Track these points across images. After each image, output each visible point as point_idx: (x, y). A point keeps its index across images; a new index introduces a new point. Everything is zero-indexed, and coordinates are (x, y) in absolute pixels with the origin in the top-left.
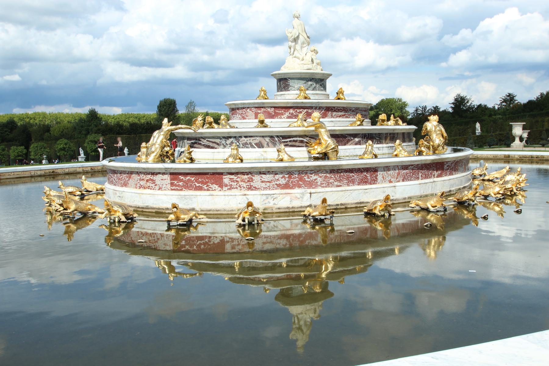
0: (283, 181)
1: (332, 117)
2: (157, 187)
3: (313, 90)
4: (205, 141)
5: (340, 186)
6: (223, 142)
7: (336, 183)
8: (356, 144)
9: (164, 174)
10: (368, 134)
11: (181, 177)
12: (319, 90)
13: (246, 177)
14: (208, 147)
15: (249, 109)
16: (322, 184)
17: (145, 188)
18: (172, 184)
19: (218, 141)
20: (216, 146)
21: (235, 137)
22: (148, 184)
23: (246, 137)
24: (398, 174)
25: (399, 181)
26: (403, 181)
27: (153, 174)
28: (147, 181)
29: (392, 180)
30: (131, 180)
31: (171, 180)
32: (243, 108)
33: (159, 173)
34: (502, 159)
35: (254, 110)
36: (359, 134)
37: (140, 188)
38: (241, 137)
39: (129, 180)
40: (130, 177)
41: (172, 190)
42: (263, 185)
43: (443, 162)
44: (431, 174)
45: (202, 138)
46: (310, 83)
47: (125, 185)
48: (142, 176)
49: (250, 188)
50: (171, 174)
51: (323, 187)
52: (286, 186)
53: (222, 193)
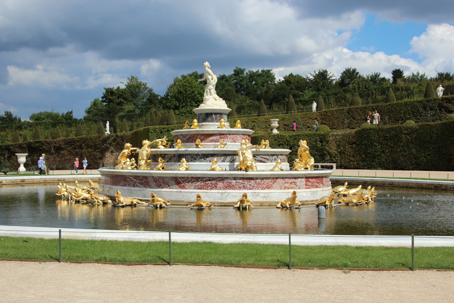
2: (297, 187)
4: (259, 157)
6: (271, 158)
9: (302, 178)
11: (310, 180)
14: (261, 161)
15: (238, 136)
17: (288, 188)
18: (306, 185)
19: (267, 157)
20: (266, 161)
21: (276, 155)
22: (291, 185)
23: (281, 155)
27: (295, 178)
28: (291, 183)
30: (275, 184)
31: (306, 181)
32: (235, 134)
33: (299, 177)
34: (97, 181)
35: (241, 136)
37: (284, 189)
38: (279, 155)
39: (273, 184)
40: (275, 181)
41: (306, 188)
45: (256, 155)
47: (268, 187)
48: (287, 180)
50: (306, 178)
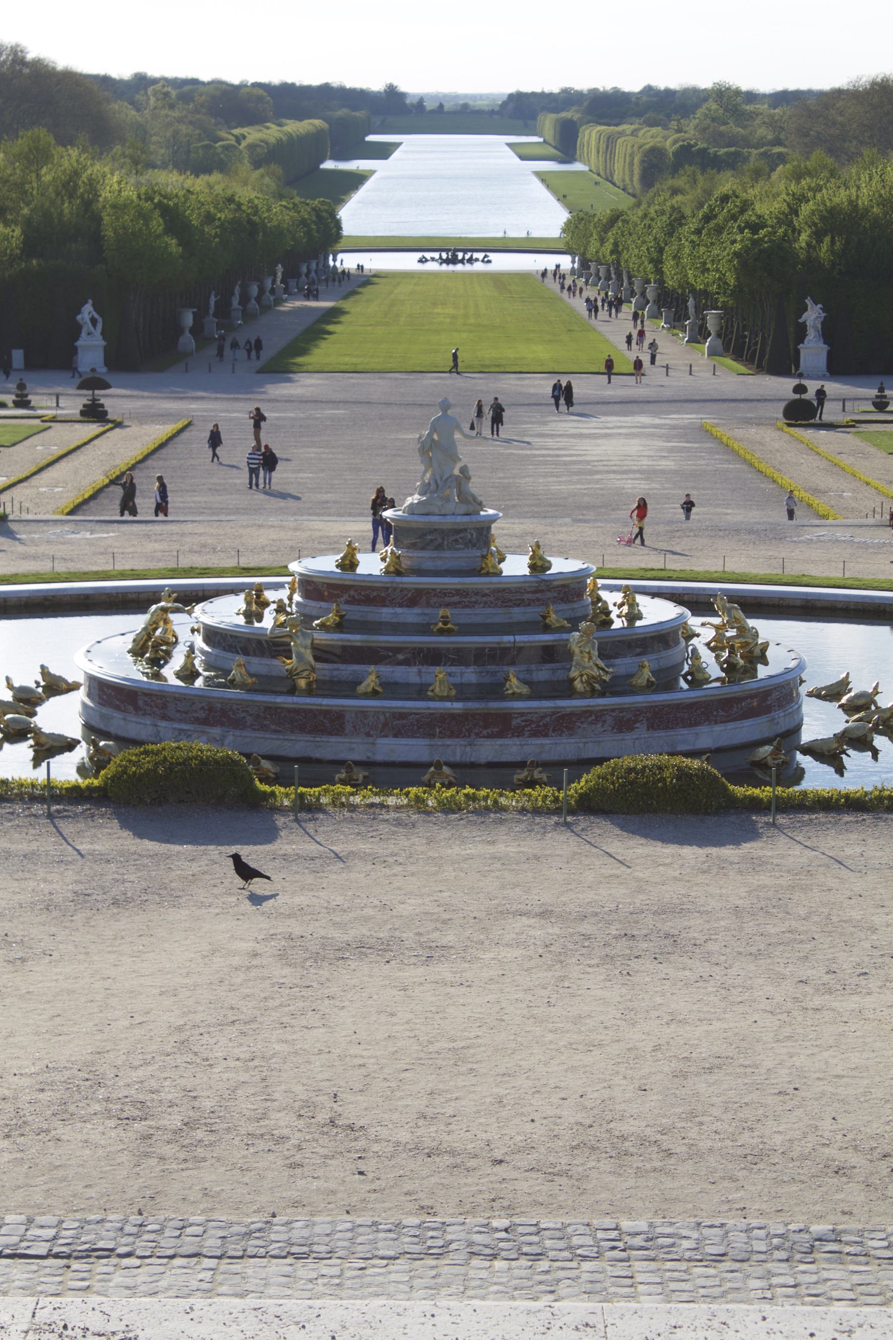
0: (201, 714)
1: (428, 605)
3: (436, 549)
5: (279, 731)
7: (273, 727)
8: (400, 663)
10: (429, 649)
12: (449, 549)
13: (159, 701)
16: (252, 725)
24: (385, 725)
25: (386, 736)
26: (395, 736)
29: (372, 732)
36: (406, 648)
42: (178, 715)
43: (510, 714)
44: (470, 731)
46: (429, 537)
49: (164, 717)
51: (254, 730)
52: (205, 722)
53: (134, 719)
